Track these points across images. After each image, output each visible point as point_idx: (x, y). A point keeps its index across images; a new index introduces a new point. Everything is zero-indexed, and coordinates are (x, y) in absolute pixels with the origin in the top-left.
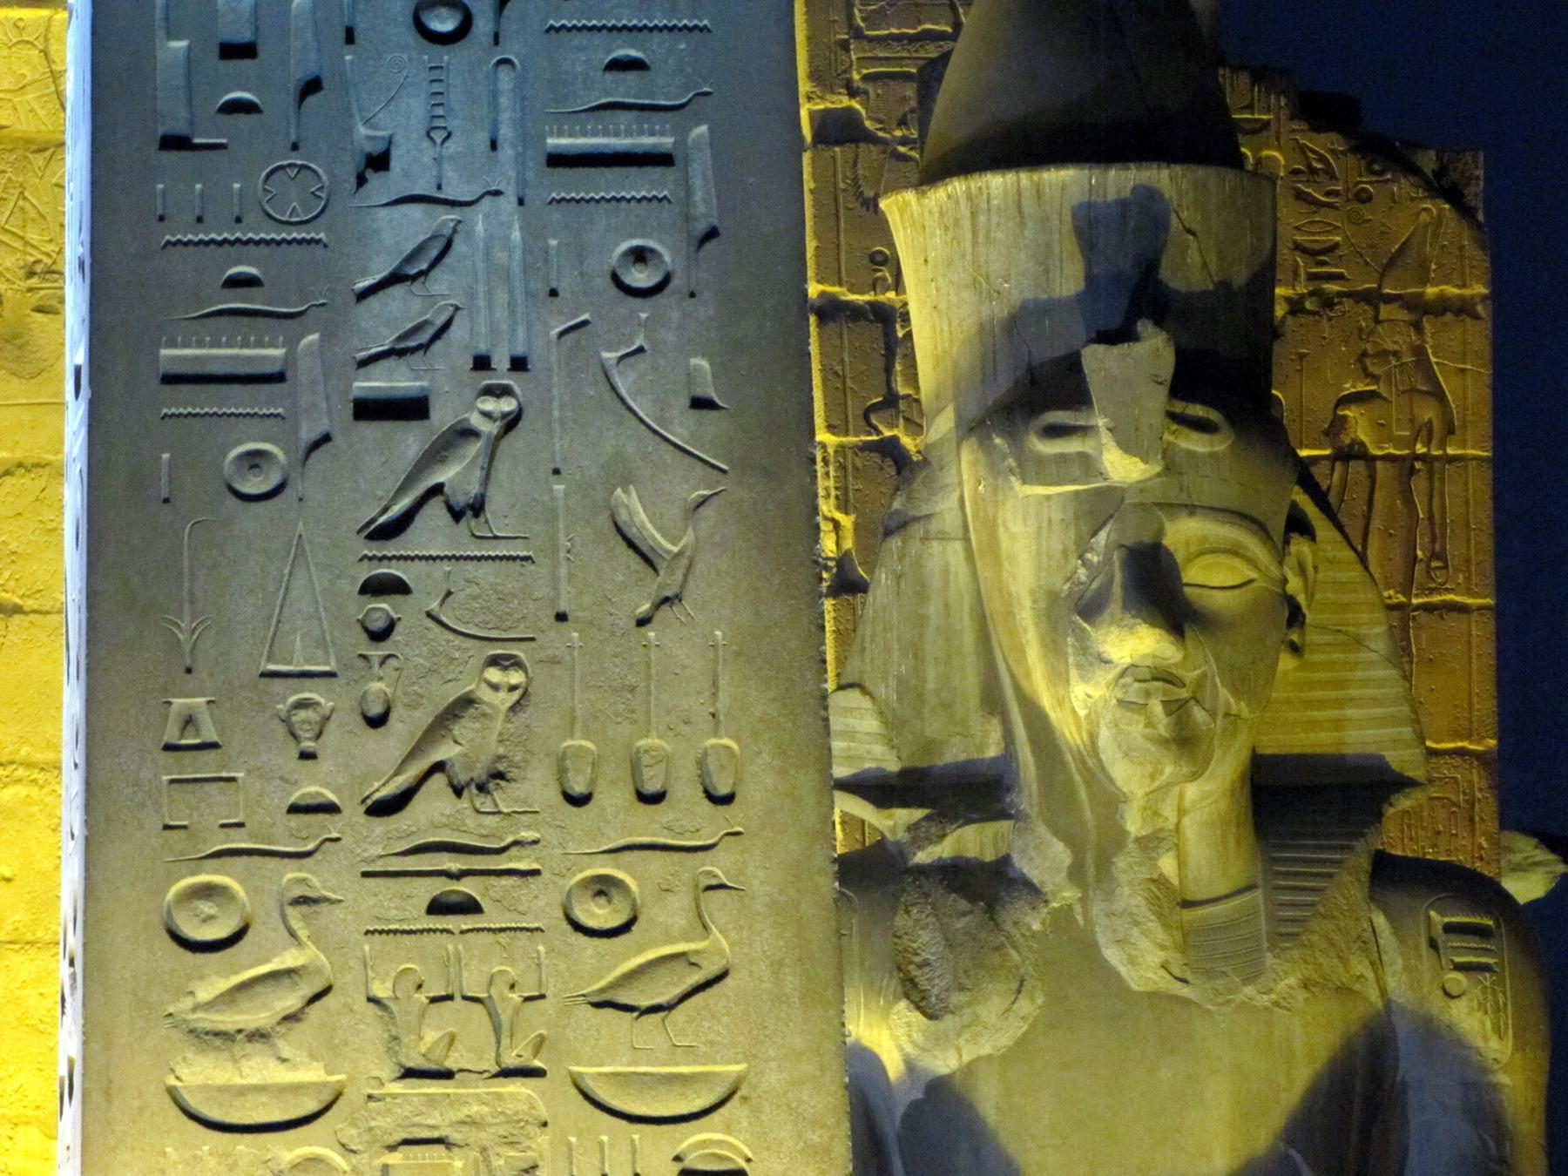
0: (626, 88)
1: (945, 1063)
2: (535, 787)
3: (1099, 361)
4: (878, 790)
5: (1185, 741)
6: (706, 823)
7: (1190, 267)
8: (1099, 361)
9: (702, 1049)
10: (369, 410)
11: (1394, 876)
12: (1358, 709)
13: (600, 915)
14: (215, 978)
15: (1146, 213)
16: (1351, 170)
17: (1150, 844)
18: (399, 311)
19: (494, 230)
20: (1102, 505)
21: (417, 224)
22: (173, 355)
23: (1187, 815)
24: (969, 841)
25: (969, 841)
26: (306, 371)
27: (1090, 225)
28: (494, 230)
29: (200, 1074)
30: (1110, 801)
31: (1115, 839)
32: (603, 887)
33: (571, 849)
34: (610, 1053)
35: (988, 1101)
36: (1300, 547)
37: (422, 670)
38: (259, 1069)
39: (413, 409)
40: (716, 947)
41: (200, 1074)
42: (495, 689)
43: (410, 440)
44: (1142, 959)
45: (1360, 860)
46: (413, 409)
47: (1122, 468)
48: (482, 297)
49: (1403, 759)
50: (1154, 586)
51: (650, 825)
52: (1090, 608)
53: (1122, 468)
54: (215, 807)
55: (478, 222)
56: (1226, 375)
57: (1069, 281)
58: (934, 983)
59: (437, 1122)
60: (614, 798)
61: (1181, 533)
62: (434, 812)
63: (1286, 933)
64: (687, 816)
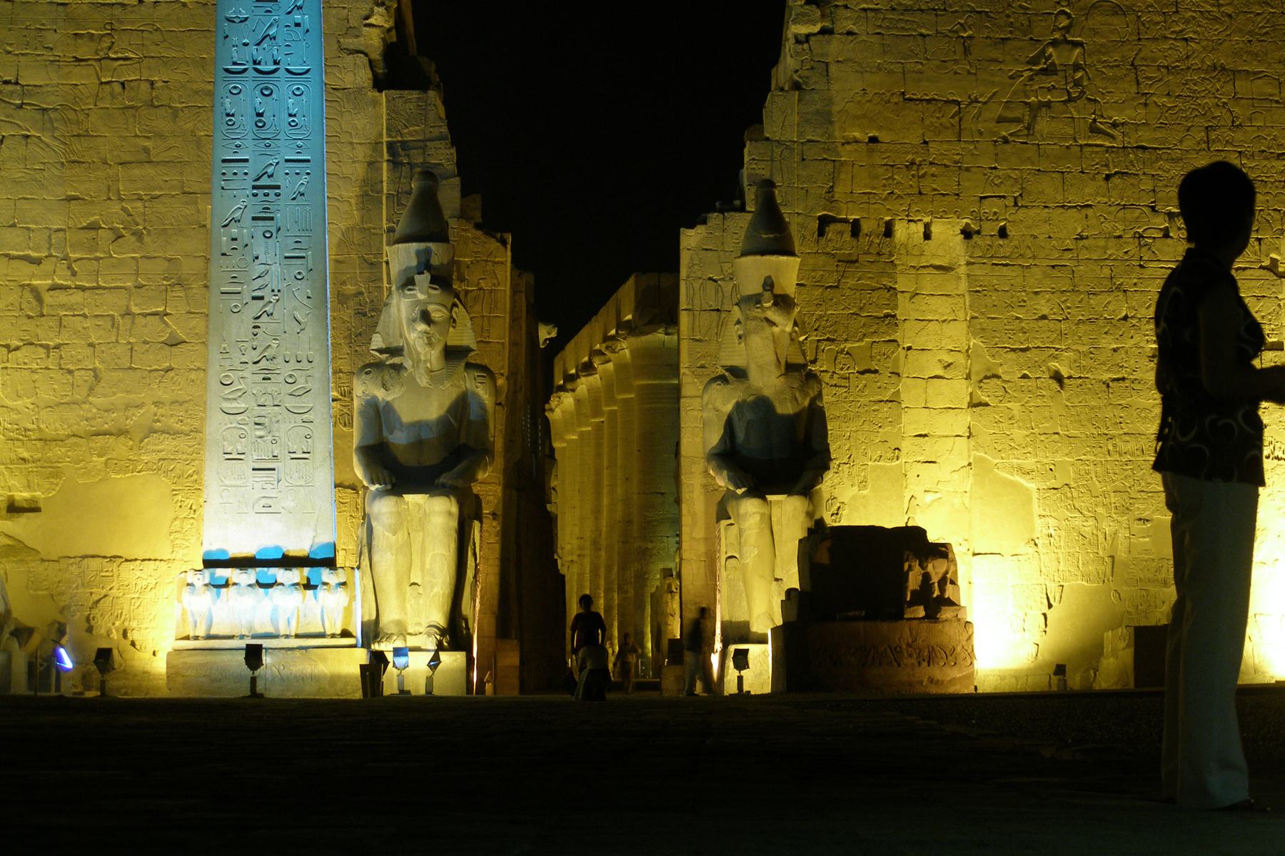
0: (298, 246)
1: (389, 399)
2: (280, 360)
3: (417, 278)
4: (380, 351)
5: (430, 344)
6: (309, 366)
7: (435, 261)
8: (417, 278)
9: (307, 402)
10: (254, 298)
11: (469, 366)
12: (464, 336)
13: (290, 380)
14: (228, 390)
15: (428, 252)
16: (483, 238)
17: (425, 361)
18: (260, 282)
19: (275, 269)
20: (418, 302)
21: (263, 268)
22: (223, 289)
23: (433, 356)
24: (396, 360)
25: (396, 360)
26: (245, 292)
27: (418, 253)
28: (275, 269)
29: (226, 405)
30: (418, 354)
31: (419, 361)
32: (291, 376)
33: (286, 370)
34: (291, 403)
35: (396, 406)
36: (455, 309)
37: (261, 341)
38: (235, 405)
39: (262, 298)
40: (309, 386)
41: (226, 405)
42: (274, 344)
43: (261, 303)
44: (423, 381)
45: (463, 364)
46: (262, 298)
47: (421, 297)
48: (273, 281)
49: (473, 346)
50: (426, 317)
51: (299, 366)
52: (414, 321)
53: (421, 297)
54: (228, 362)
55: (273, 268)
56: (441, 280)
57: (414, 263)
58: (389, 385)
59: (263, 413)
60: (293, 361)
61: (431, 308)
62: (263, 364)
63: (449, 376)
64: (305, 364)
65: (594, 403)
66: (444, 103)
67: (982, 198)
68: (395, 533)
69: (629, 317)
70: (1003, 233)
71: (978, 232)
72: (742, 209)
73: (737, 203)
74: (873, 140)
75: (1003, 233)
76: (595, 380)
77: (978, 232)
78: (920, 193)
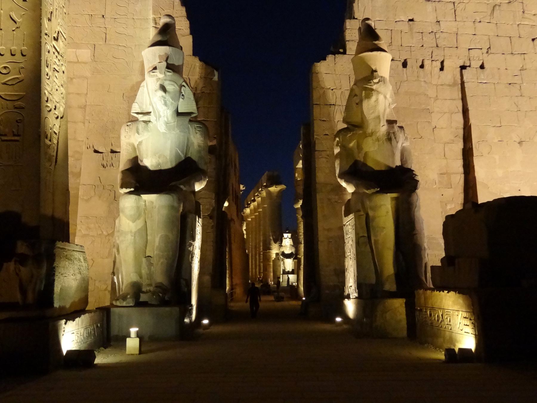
13: (4, 71)
24: (146, 118)
25: (146, 118)
31: (160, 116)
47: (161, 76)
65: (255, 210)
66: (190, 16)
67: (469, 49)
68: (134, 221)
69: (265, 184)
70: (482, 67)
71: (469, 66)
72: (344, 53)
73: (341, 50)
74: (412, 20)
75: (482, 67)
76: (256, 203)
77: (469, 66)
78: (437, 46)
